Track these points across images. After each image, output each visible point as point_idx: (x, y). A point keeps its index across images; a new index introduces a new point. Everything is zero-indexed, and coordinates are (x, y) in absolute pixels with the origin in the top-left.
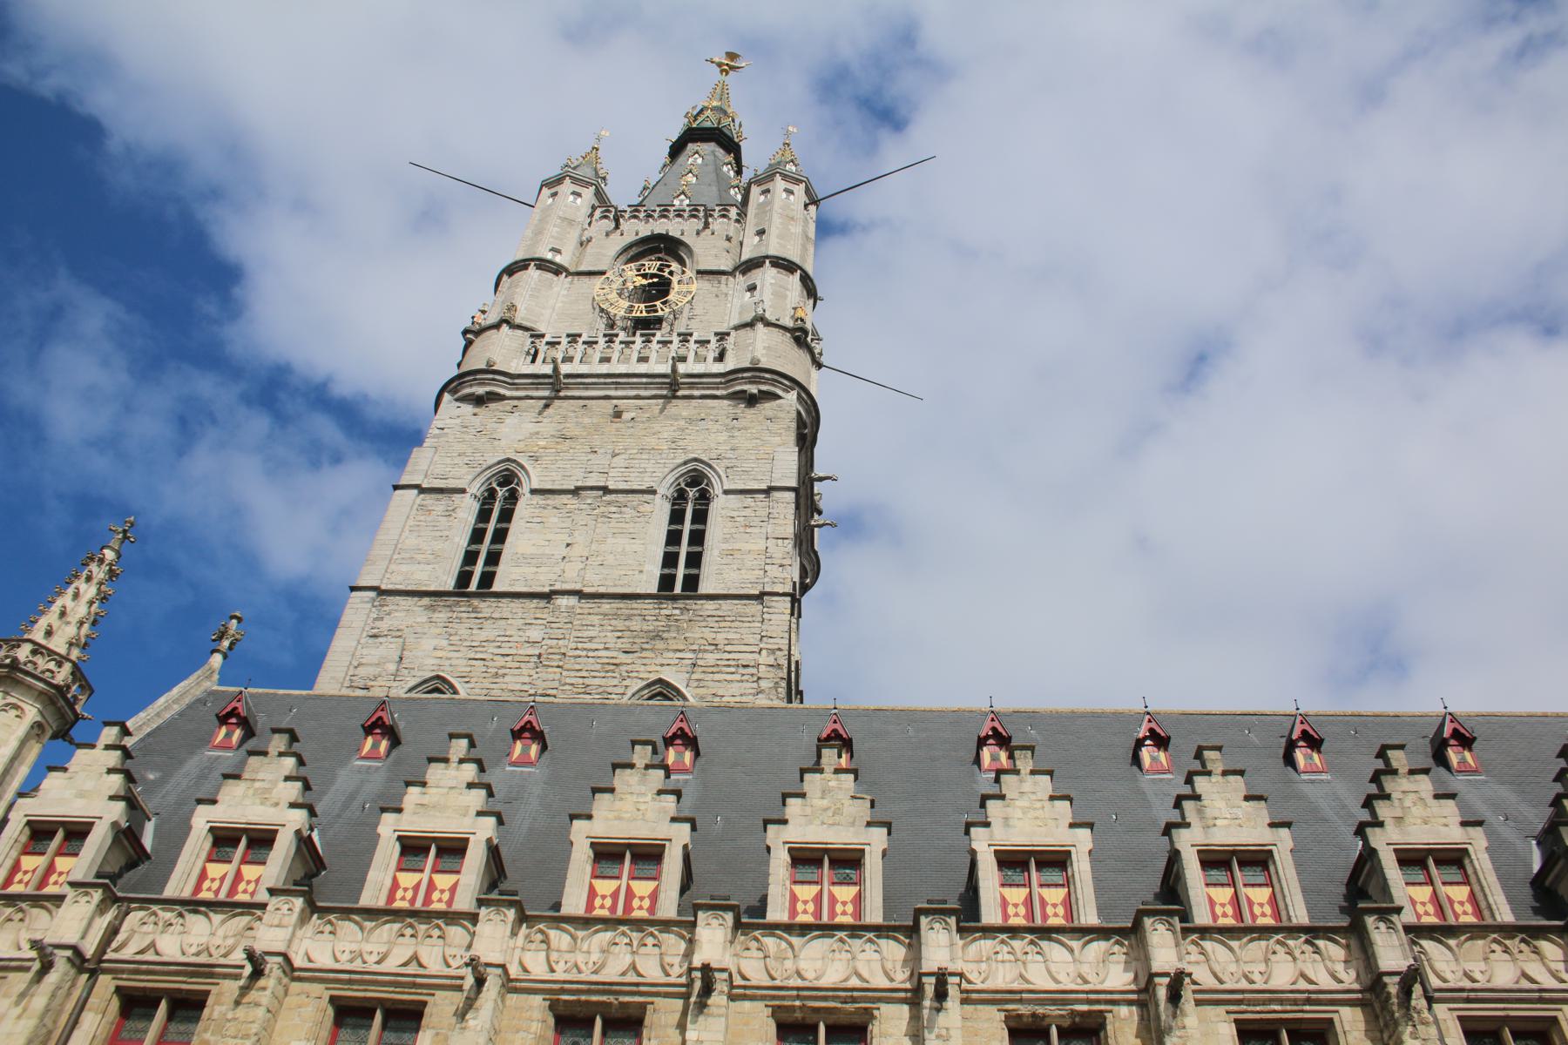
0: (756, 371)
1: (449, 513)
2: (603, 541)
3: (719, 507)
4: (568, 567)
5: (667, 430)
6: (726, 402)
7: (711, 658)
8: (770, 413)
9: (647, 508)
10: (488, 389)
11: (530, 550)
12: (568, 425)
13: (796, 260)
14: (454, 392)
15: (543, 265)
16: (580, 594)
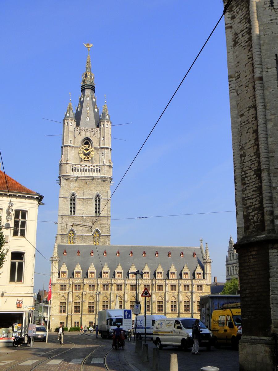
0: (105, 177)
1: (67, 201)
2: (87, 207)
3: (101, 201)
4: (84, 211)
5: (93, 186)
6: (101, 181)
7: (102, 225)
8: (107, 183)
9: (92, 201)
10: (68, 178)
11: (79, 208)
12: (80, 185)
13: (109, 147)
14: (62, 177)
15: (70, 146)
16: (86, 216)
